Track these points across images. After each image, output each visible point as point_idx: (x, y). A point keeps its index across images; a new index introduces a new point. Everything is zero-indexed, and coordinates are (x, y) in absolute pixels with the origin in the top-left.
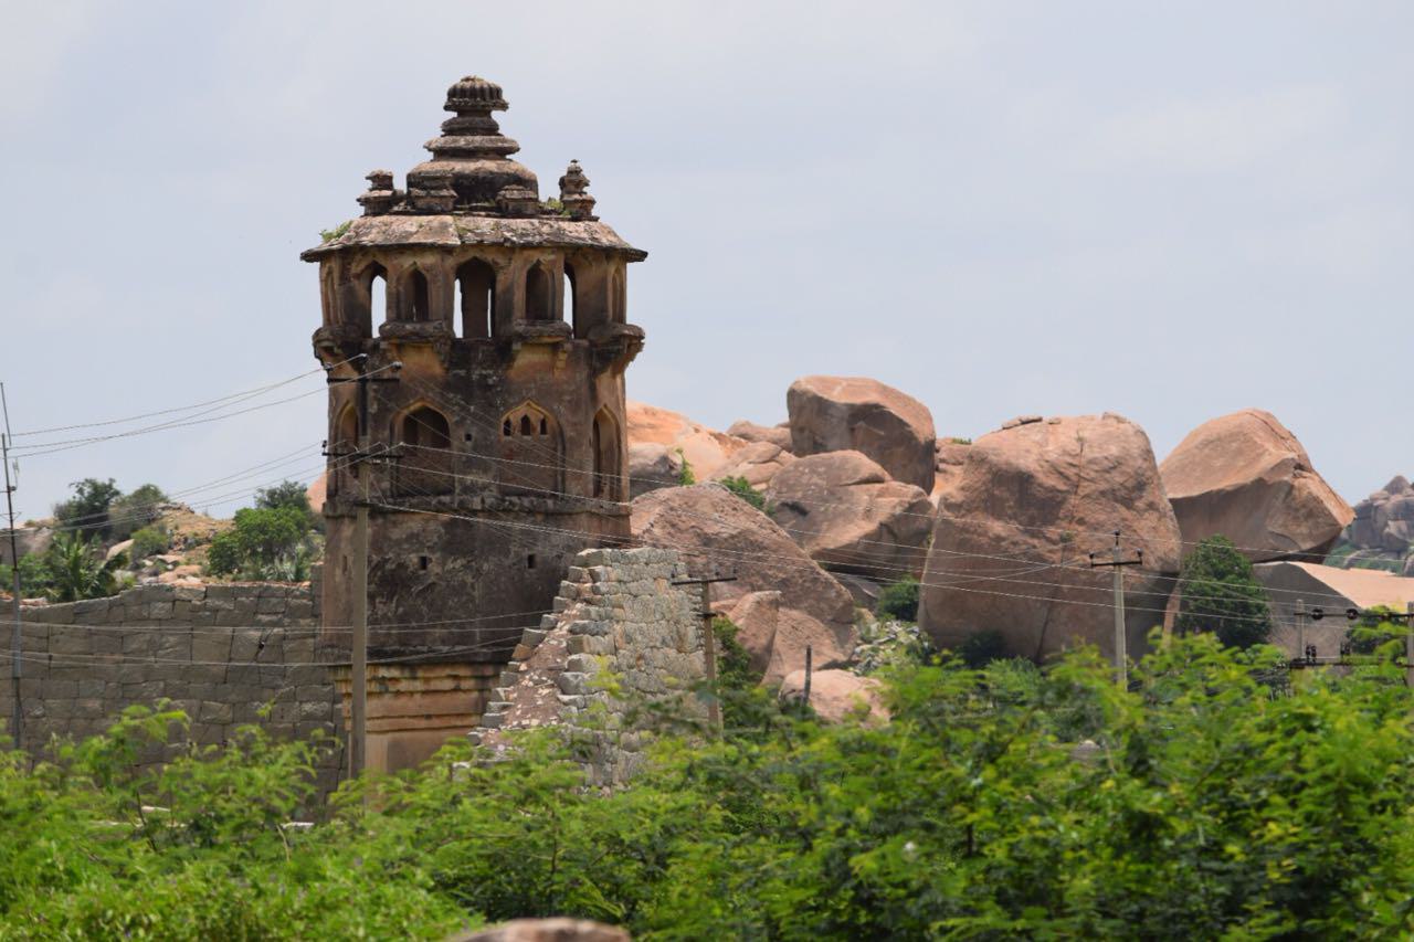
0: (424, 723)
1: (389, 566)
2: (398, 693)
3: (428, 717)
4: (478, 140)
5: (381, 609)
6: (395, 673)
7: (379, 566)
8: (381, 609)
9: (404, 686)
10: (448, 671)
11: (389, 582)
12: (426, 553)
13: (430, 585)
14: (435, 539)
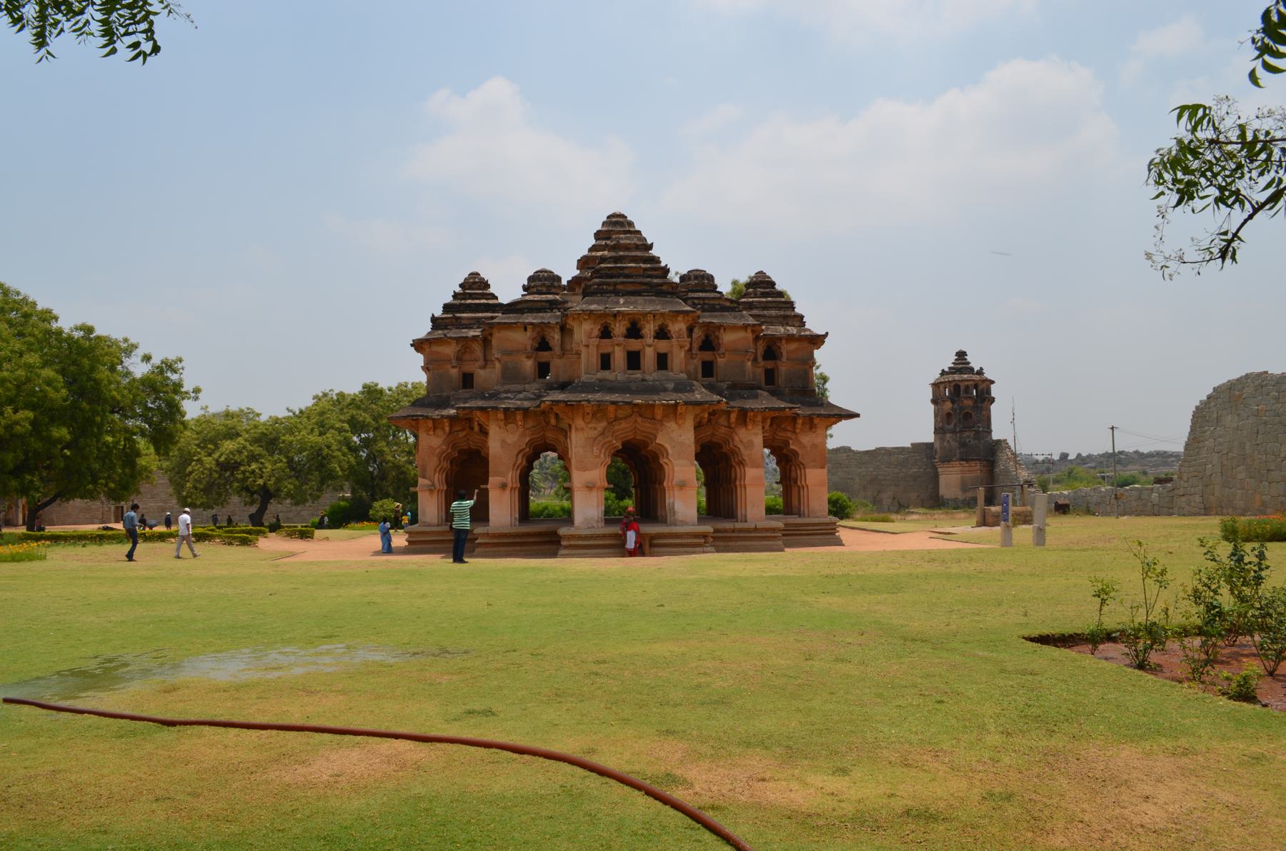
4: (964, 361)
11: (963, 445)
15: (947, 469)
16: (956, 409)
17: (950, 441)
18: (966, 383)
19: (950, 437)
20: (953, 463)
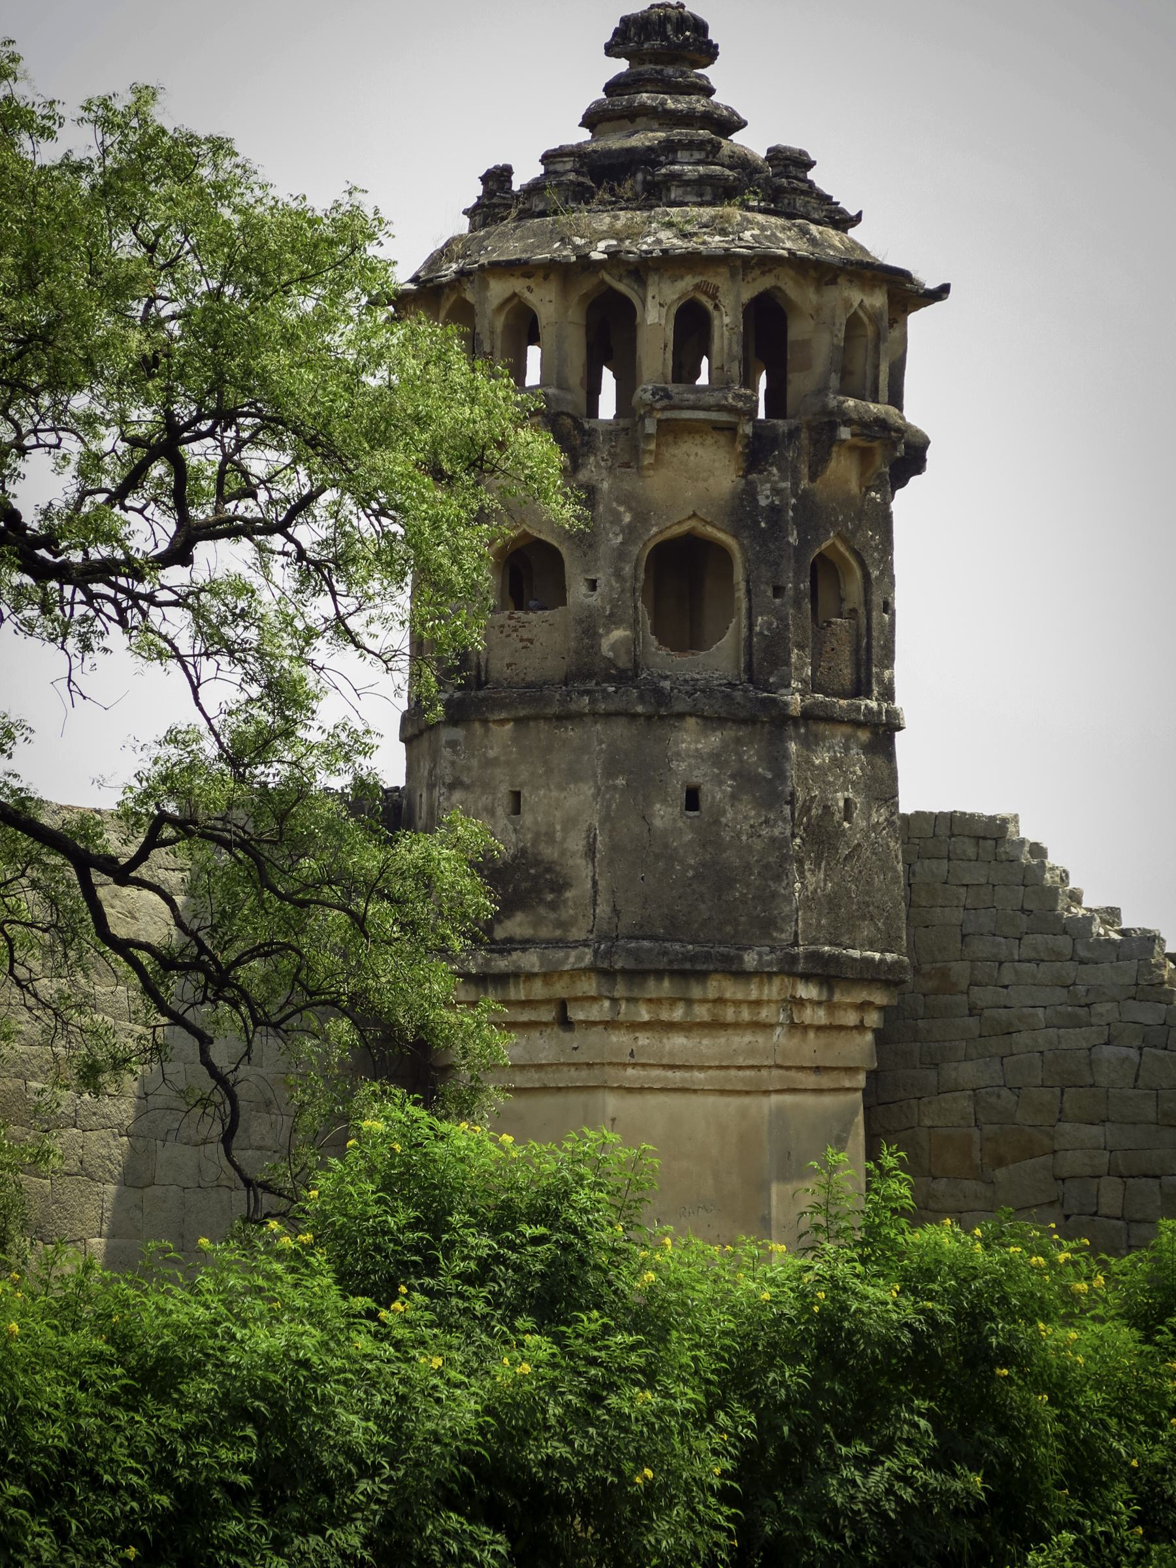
0: (810, 1080)
3: (817, 1069)
9: (809, 1015)
10: (862, 995)
14: (859, 773)
15: (644, 1039)
16: (775, 512)
17: (714, 794)
18: (856, 296)
19: (716, 758)
20: (714, 987)
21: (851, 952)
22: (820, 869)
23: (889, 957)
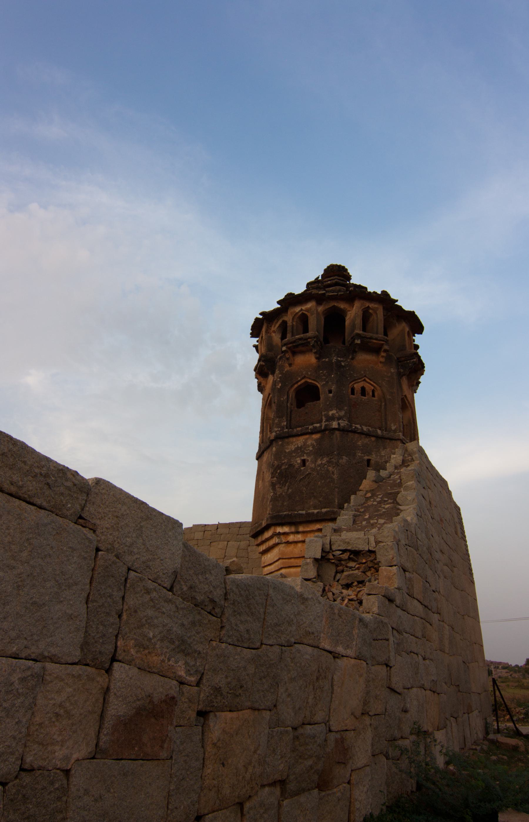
1: (283, 467)
2: (288, 543)
5: (279, 491)
6: (286, 529)
7: (279, 467)
8: (279, 491)
9: (291, 538)
12: (305, 457)
13: (308, 474)
14: (311, 449)
21: (301, 512)
22: (285, 486)
23: (324, 510)
